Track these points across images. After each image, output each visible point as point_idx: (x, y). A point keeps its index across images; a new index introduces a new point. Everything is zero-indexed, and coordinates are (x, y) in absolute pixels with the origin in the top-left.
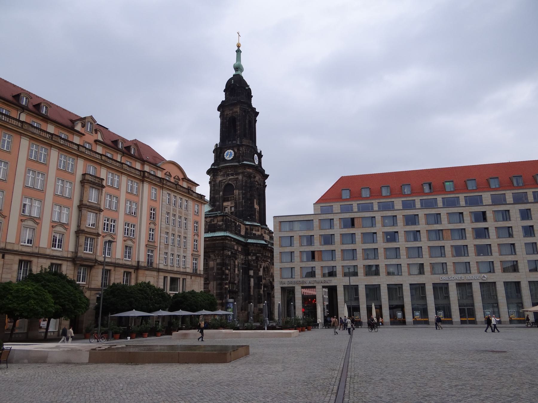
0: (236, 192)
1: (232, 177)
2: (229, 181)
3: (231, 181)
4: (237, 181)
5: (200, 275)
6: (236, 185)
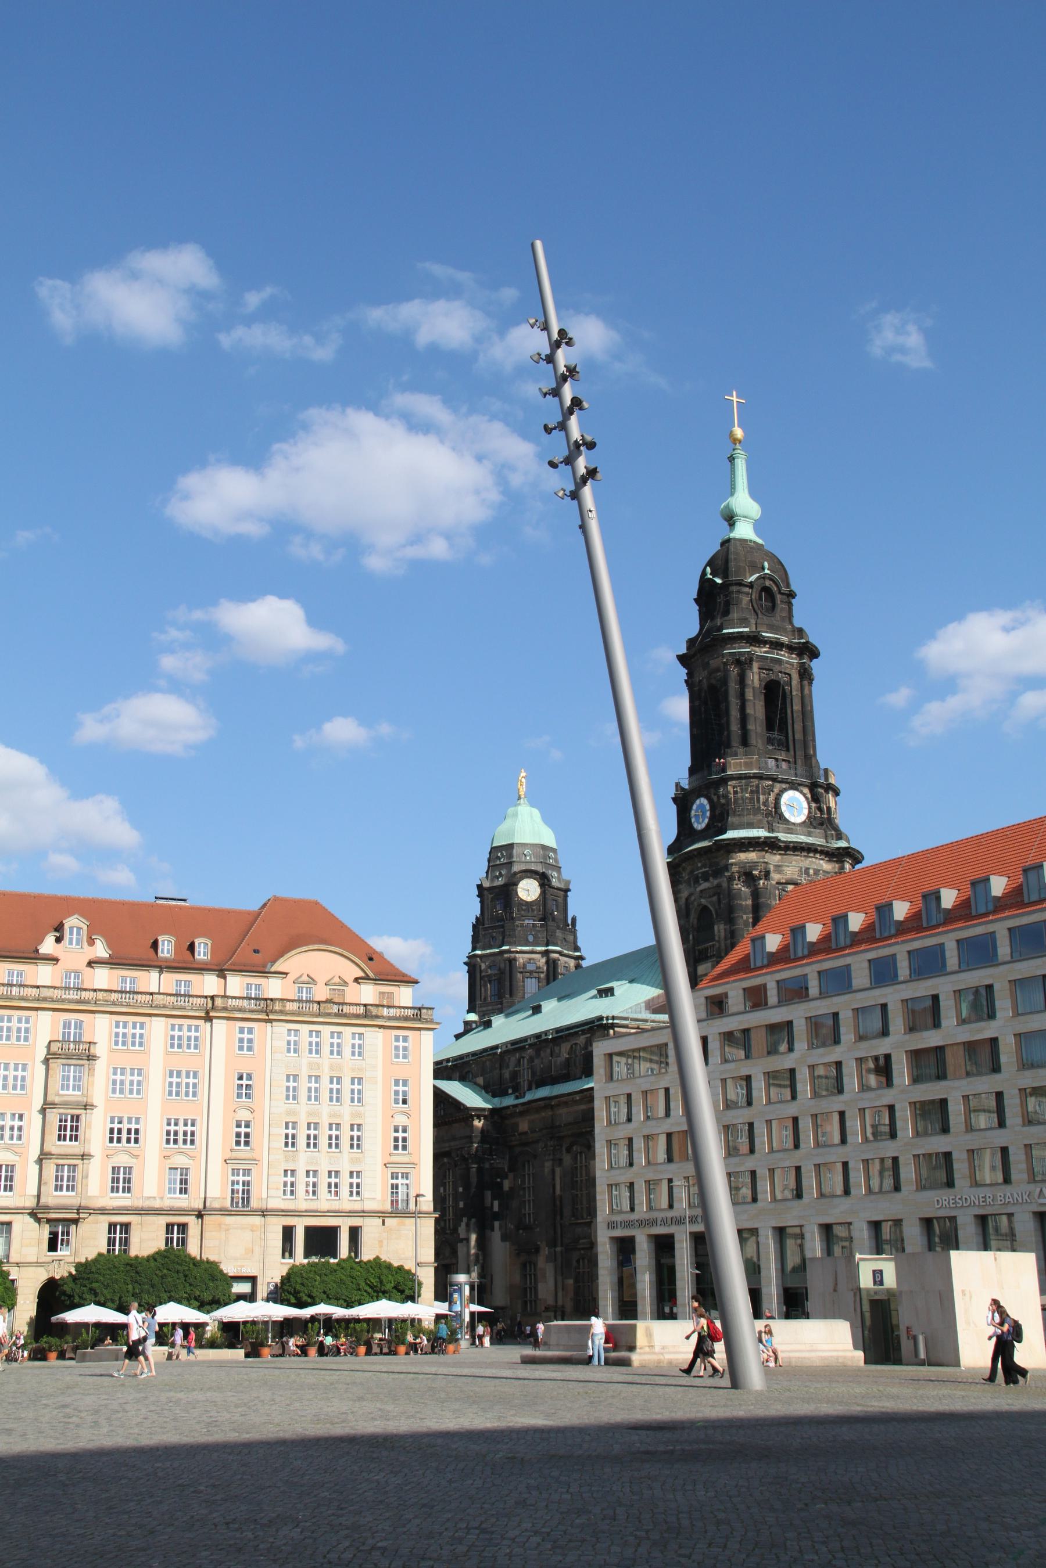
0: (719, 931)
1: (705, 885)
2: (701, 897)
3: (704, 898)
4: (719, 894)
5: (417, 1214)
6: (717, 907)
